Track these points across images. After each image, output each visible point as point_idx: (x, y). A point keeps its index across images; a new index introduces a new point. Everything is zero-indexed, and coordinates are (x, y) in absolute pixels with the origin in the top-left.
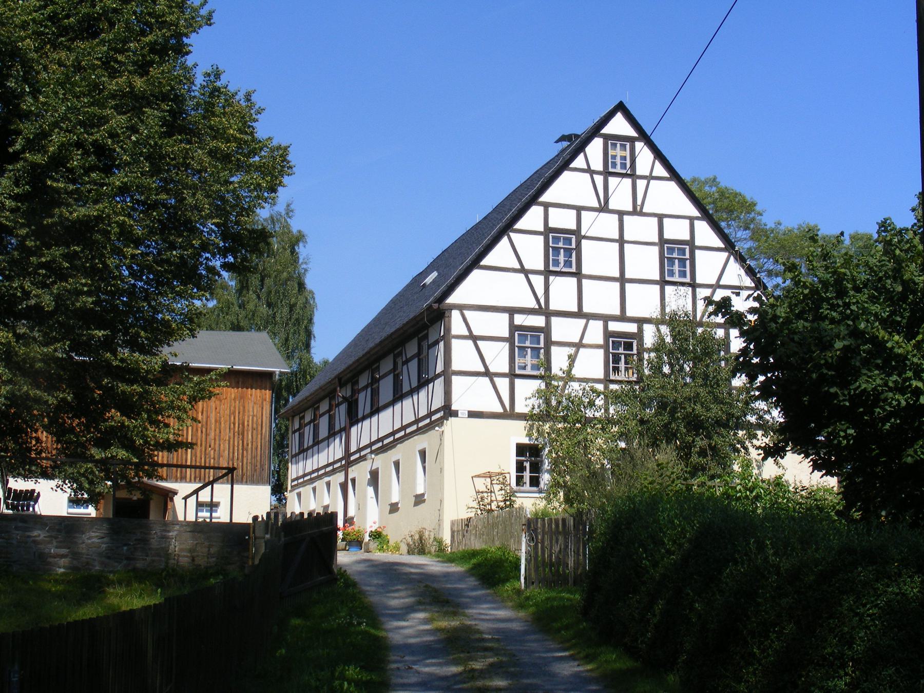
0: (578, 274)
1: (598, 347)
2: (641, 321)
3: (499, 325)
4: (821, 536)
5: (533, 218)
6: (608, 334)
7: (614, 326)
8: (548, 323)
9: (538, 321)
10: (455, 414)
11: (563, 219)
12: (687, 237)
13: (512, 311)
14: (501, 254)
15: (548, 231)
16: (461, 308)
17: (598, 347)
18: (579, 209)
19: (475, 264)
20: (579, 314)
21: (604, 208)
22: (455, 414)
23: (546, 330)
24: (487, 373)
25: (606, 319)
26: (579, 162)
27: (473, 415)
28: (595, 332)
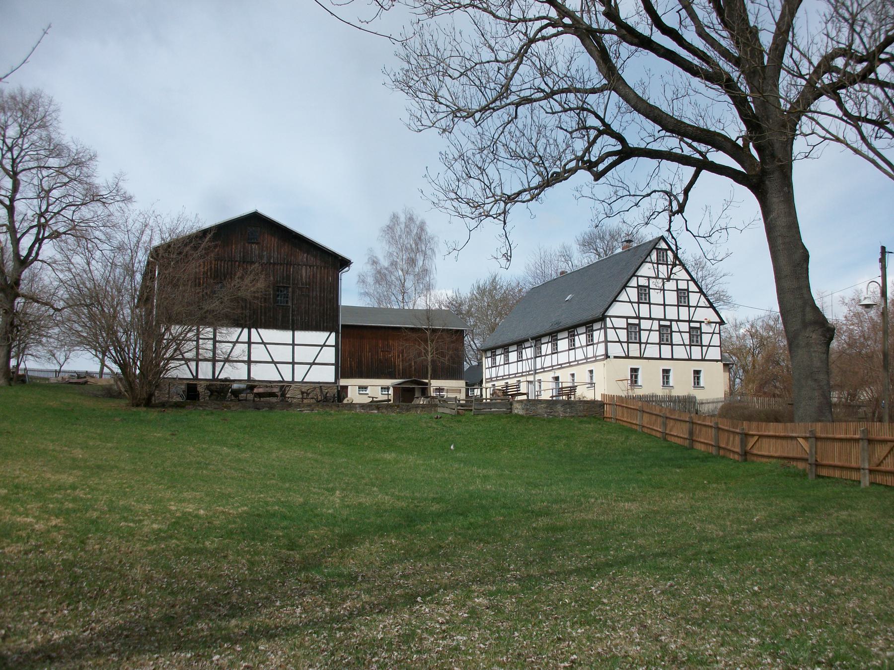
0: (650, 304)
1: (332, 364)
2: (671, 321)
3: (622, 323)
4: (402, 647)
5: (634, 282)
6: (660, 326)
7: (662, 323)
8: (640, 322)
9: (636, 321)
10: (609, 357)
11: (643, 282)
12: (647, 284)
13: (627, 318)
14: (623, 297)
15: (639, 287)
16: (610, 317)
17: (332, 364)
18: (649, 278)
19: (615, 300)
20: (650, 318)
21: (657, 277)
22: (609, 357)
23: (639, 325)
24: (620, 342)
25: (659, 320)
26: (648, 259)
27: (615, 357)
28: (656, 326)
